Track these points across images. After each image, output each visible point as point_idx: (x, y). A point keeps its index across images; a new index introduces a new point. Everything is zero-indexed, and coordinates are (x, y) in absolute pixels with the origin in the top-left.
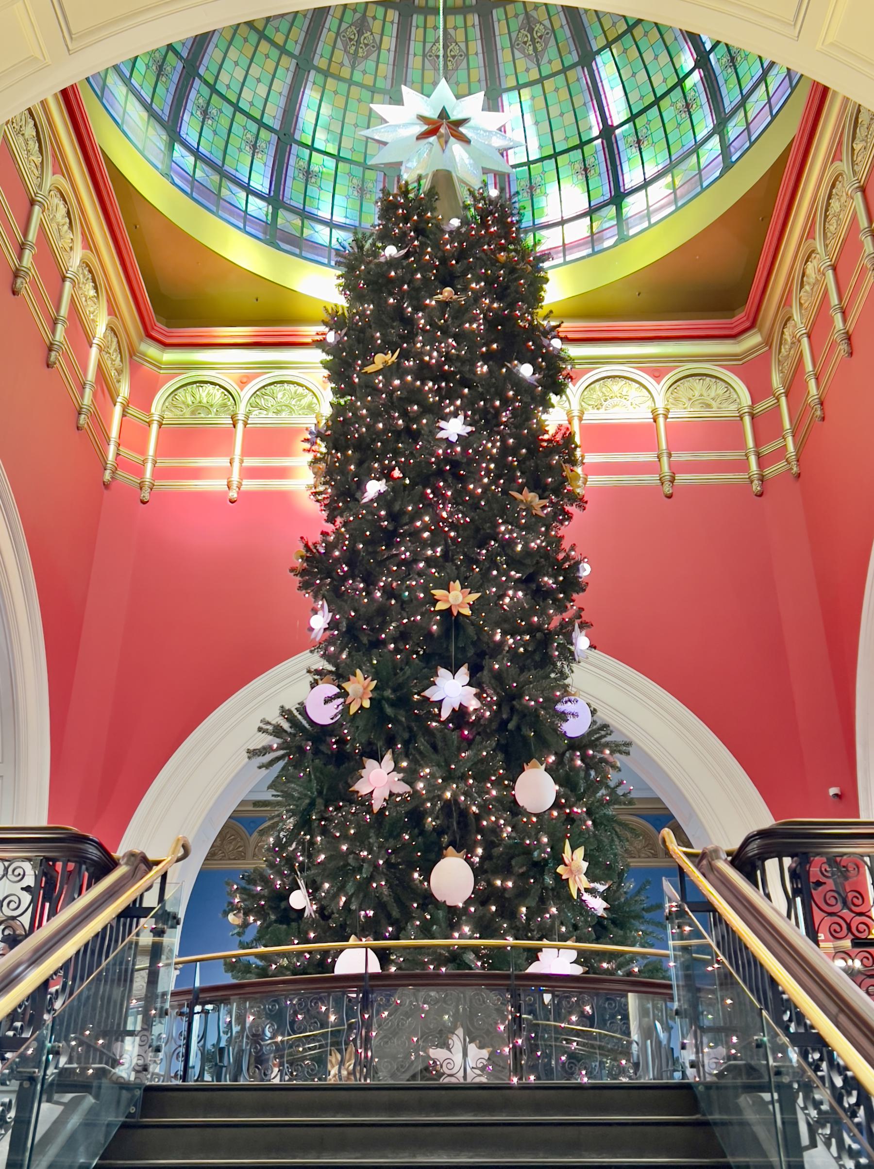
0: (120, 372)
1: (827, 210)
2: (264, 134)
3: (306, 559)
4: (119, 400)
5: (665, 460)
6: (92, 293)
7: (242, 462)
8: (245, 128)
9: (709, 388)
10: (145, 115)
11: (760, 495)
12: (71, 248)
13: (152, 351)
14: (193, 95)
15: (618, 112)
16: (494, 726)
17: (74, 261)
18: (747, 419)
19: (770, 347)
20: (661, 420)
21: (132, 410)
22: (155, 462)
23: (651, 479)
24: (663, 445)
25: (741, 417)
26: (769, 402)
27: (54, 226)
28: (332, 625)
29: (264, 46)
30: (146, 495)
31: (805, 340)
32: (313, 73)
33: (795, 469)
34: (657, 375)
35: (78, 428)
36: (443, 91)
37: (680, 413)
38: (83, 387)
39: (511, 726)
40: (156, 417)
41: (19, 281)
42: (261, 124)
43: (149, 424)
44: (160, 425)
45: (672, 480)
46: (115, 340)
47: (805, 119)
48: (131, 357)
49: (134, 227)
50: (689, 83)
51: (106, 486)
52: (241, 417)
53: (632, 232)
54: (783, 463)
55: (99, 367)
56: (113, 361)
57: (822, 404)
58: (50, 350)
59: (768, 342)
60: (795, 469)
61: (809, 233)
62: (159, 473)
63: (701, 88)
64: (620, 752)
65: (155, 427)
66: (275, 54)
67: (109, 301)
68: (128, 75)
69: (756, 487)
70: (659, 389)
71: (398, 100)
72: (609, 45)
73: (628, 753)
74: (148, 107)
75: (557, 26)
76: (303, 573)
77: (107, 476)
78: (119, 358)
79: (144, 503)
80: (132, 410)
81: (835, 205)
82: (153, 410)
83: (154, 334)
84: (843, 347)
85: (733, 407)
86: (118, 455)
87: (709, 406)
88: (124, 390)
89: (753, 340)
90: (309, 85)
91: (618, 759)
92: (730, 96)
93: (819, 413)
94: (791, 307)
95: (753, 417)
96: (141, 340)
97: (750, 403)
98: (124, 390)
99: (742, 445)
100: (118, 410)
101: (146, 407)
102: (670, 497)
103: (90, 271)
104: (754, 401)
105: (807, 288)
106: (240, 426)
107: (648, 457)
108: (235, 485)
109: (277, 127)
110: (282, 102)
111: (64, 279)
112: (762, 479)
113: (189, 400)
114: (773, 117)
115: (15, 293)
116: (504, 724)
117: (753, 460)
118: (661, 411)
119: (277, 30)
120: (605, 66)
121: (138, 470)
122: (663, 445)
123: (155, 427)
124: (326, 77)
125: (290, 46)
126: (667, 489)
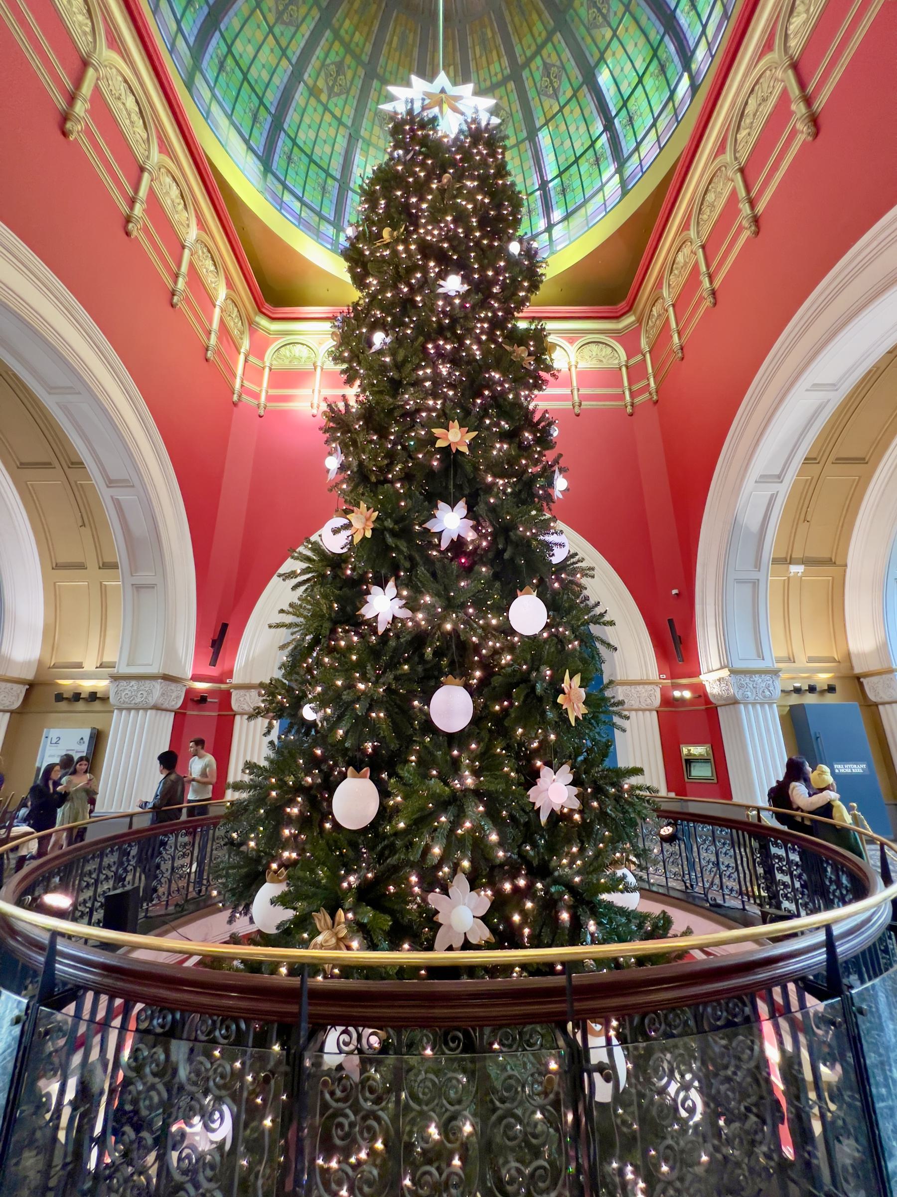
0: (242, 333)
1: (702, 204)
2: (330, 181)
3: (332, 419)
4: (243, 350)
5: (575, 392)
6: (212, 268)
7: (320, 392)
8: (317, 174)
9: (602, 350)
10: (244, 147)
11: (631, 415)
12: (188, 225)
13: (263, 322)
14: (280, 143)
15: (551, 171)
16: (491, 555)
17: (191, 234)
18: (624, 369)
20: (573, 369)
21: (252, 359)
22: (267, 392)
23: (567, 405)
24: (575, 384)
25: (620, 369)
26: (639, 357)
27: (169, 202)
28: (342, 468)
30: (262, 412)
31: (671, 309)
32: (360, 141)
33: (655, 398)
34: (571, 341)
35: (207, 360)
36: (442, 79)
37: (583, 365)
38: (209, 333)
39: (506, 556)
40: (267, 364)
41: (130, 226)
43: (264, 368)
44: (270, 369)
45: (580, 405)
46: (236, 310)
47: (697, 128)
48: (250, 325)
49: (242, 229)
50: (598, 145)
51: (235, 404)
52: (319, 364)
53: (558, 248)
54: (647, 394)
55: (222, 322)
56: (235, 325)
57: (682, 349)
58: (173, 294)
59: (639, 320)
60: (655, 398)
61: (686, 226)
62: (270, 398)
63: (607, 145)
64: (586, 575)
65: (267, 370)
66: (335, 123)
67: (227, 278)
68: (230, 113)
70: (572, 349)
71: (408, 84)
72: (546, 123)
73: (593, 577)
74: (247, 142)
75: (514, 111)
76: (326, 430)
77: (235, 398)
78: (240, 323)
79: (261, 417)
80: (252, 359)
81: (710, 197)
82: (266, 359)
83: (264, 310)
84: (708, 302)
85: (616, 362)
86: (242, 386)
87: (601, 361)
88: (245, 345)
89: (630, 319)
90: (358, 150)
91: (584, 581)
92: (628, 145)
93: (680, 355)
94: (661, 288)
95: (627, 367)
96: (256, 314)
98: (245, 345)
100: (242, 358)
101: (261, 357)
102: (578, 415)
103: (209, 251)
105: (676, 272)
106: (319, 370)
107: (567, 391)
108: (315, 406)
109: (338, 177)
110: (341, 160)
111: (183, 247)
112: (632, 405)
113: (288, 354)
114: (661, 149)
116: (499, 554)
118: (573, 363)
119: (336, 105)
120: (544, 138)
121: (257, 396)
122: (575, 384)
123: (267, 370)
124: (369, 145)
126: (577, 410)
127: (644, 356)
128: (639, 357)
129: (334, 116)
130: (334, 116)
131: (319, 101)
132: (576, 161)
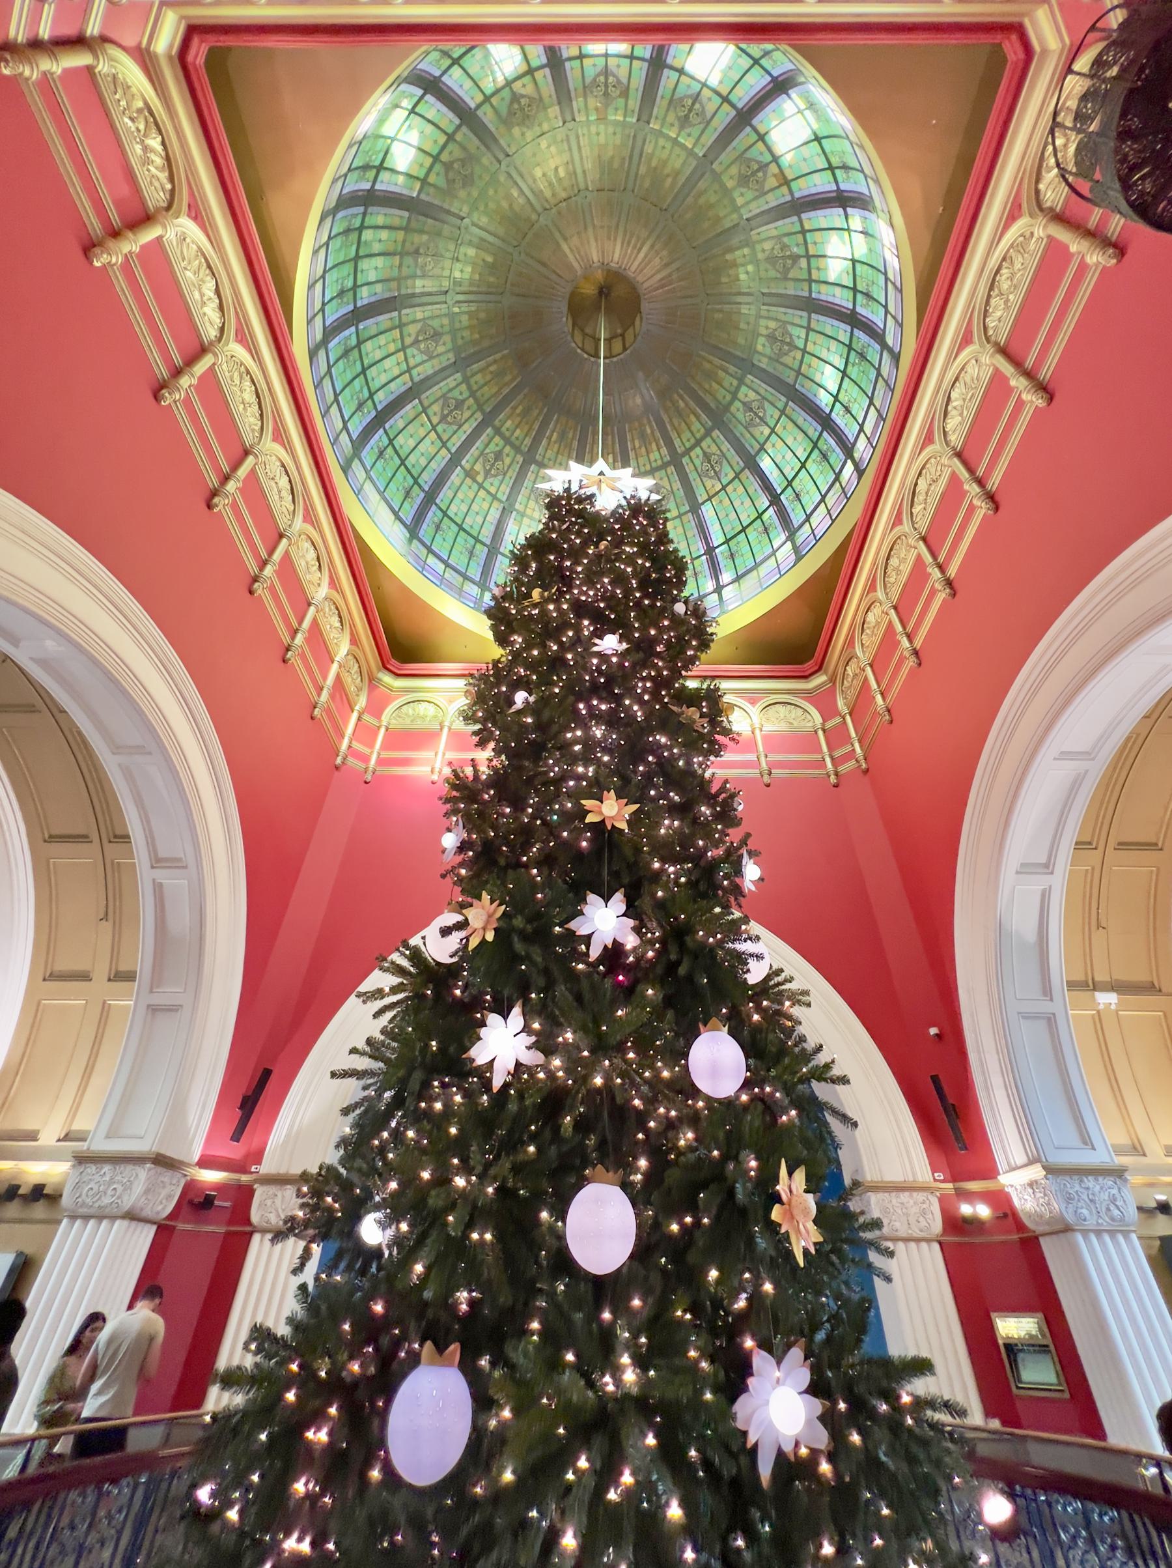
0: (360, 689)
1: (886, 568)
2: (478, 546)
3: (454, 787)
4: (357, 708)
5: (763, 759)
6: (338, 624)
7: (444, 754)
9: (790, 712)
10: (393, 517)
11: (836, 786)
12: (319, 585)
13: (387, 678)
14: (430, 514)
15: (717, 538)
16: (659, 970)
17: (320, 592)
18: (820, 733)
19: (834, 683)
20: (757, 732)
21: (366, 717)
22: (379, 754)
23: (753, 773)
24: (761, 748)
25: (816, 732)
26: (838, 720)
27: (303, 564)
28: (462, 847)
29: (482, 493)
30: (369, 777)
31: (868, 669)
32: (514, 513)
33: (864, 766)
34: (753, 702)
35: (312, 718)
36: (601, 465)
37: (769, 727)
38: (320, 690)
40: (384, 723)
41: (256, 585)
42: (477, 540)
43: (379, 728)
44: (387, 729)
45: (770, 774)
46: (356, 665)
48: (370, 681)
49: (377, 588)
50: (765, 517)
51: (337, 768)
52: (447, 724)
53: (730, 608)
54: (853, 762)
55: (338, 677)
56: (352, 681)
57: (889, 711)
58: (288, 650)
59: (832, 680)
60: (864, 766)
61: (871, 587)
62: (381, 762)
63: (775, 517)
64: (799, 1002)
65: (383, 730)
66: (489, 498)
67: (352, 634)
69: (833, 779)
70: (754, 711)
71: (567, 468)
72: (710, 499)
73: (809, 1005)
74: (396, 514)
75: (675, 488)
76: (448, 800)
77: (339, 760)
79: (366, 783)
80: (366, 717)
81: (894, 562)
82: (383, 718)
84: (911, 662)
85: (810, 724)
86: (350, 747)
88: (361, 702)
89: (820, 679)
90: (512, 520)
91: (796, 1011)
92: (797, 517)
93: (887, 717)
95: (824, 731)
96: (379, 670)
97: (821, 721)
98: (361, 702)
99: (820, 751)
100: (355, 716)
101: (378, 715)
102: (768, 785)
103: (337, 609)
104: (825, 721)
106: (446, 730)
107: (751, 757)
108: (437, 770)
109: (488, 543)
110: (492, 528)
111: (309, 604)
112: (836, 774)
113: (411, 712)
115: (251, 592)
117: (828, 760)
118: (757, 726)
120: (707, 510)
121: (365, 759)
122: (761, 748)
123: (383, 730)
125: (499, 495)
126: (766, 779)
127: (844, 718)
128: (838, 720)
129: (488, 492)
130: (488, 492)
131: (474, 480)
132: (744, 530)
